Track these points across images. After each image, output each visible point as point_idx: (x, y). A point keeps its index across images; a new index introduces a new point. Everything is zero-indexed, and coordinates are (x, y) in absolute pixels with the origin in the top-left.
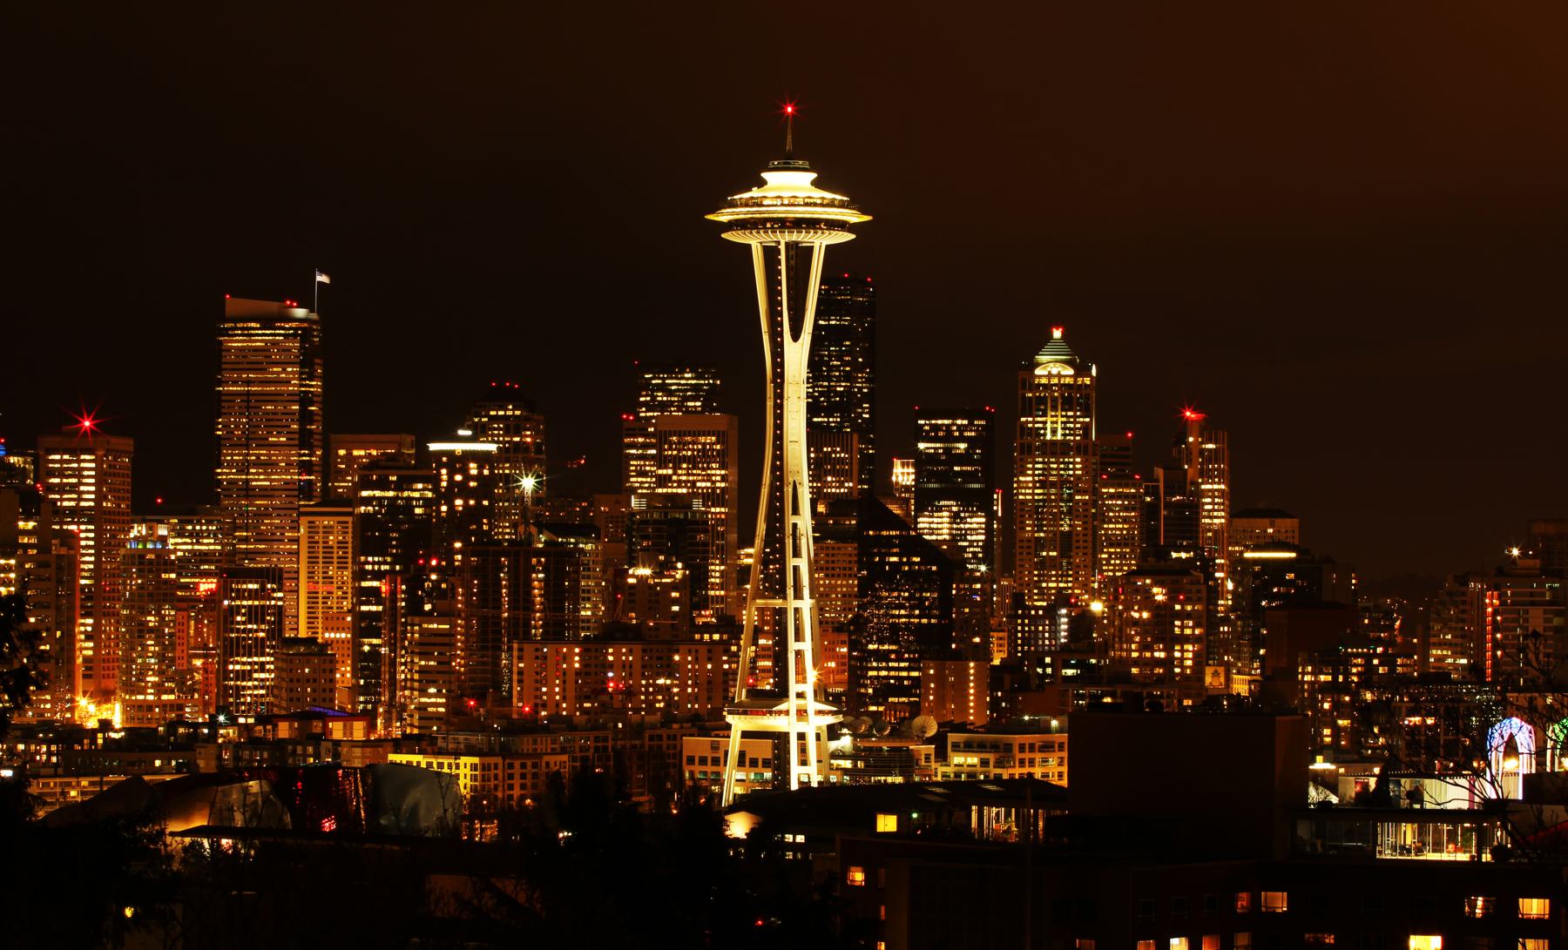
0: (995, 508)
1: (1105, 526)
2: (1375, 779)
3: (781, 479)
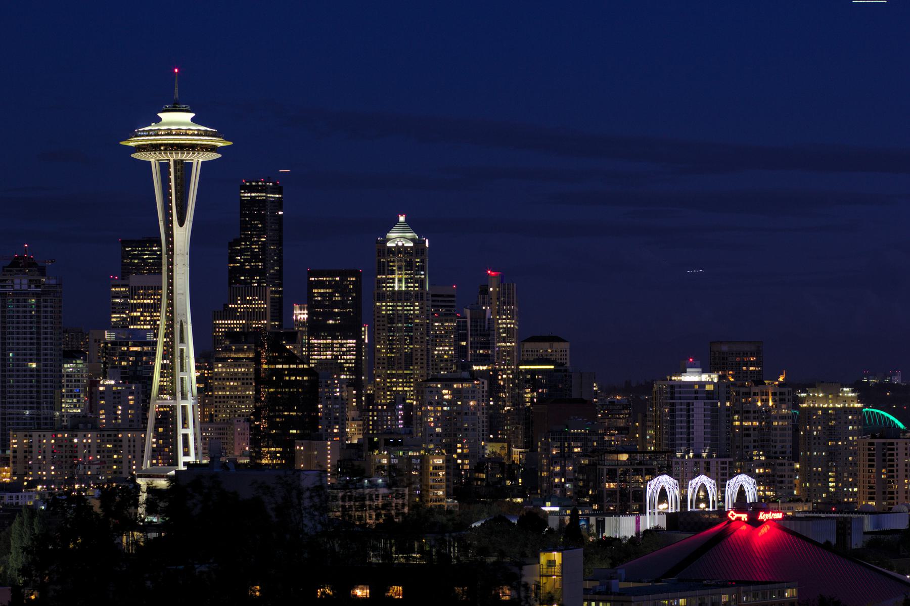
0: (363, 337)
1: (437, 348)
2: (569, 517)
3: (172, 320)
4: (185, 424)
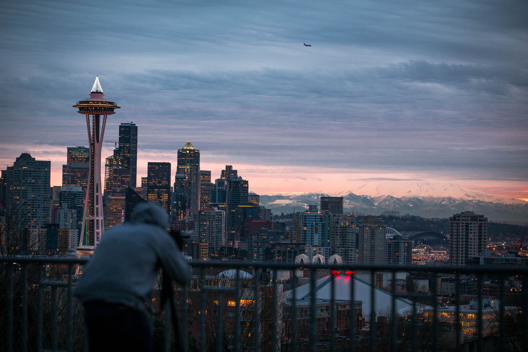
3: (93, 183)
4: (98, 228)
